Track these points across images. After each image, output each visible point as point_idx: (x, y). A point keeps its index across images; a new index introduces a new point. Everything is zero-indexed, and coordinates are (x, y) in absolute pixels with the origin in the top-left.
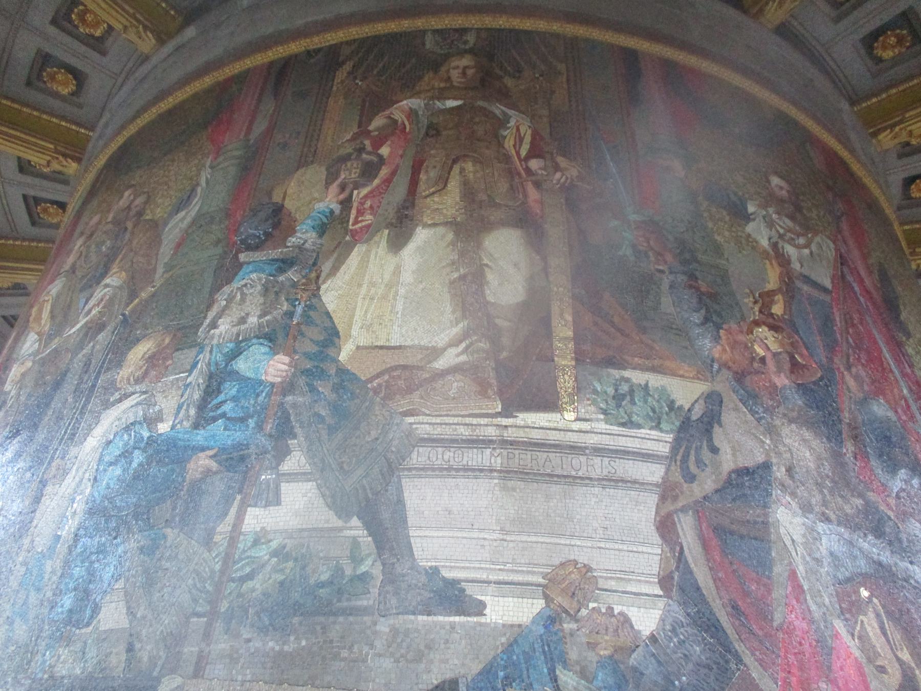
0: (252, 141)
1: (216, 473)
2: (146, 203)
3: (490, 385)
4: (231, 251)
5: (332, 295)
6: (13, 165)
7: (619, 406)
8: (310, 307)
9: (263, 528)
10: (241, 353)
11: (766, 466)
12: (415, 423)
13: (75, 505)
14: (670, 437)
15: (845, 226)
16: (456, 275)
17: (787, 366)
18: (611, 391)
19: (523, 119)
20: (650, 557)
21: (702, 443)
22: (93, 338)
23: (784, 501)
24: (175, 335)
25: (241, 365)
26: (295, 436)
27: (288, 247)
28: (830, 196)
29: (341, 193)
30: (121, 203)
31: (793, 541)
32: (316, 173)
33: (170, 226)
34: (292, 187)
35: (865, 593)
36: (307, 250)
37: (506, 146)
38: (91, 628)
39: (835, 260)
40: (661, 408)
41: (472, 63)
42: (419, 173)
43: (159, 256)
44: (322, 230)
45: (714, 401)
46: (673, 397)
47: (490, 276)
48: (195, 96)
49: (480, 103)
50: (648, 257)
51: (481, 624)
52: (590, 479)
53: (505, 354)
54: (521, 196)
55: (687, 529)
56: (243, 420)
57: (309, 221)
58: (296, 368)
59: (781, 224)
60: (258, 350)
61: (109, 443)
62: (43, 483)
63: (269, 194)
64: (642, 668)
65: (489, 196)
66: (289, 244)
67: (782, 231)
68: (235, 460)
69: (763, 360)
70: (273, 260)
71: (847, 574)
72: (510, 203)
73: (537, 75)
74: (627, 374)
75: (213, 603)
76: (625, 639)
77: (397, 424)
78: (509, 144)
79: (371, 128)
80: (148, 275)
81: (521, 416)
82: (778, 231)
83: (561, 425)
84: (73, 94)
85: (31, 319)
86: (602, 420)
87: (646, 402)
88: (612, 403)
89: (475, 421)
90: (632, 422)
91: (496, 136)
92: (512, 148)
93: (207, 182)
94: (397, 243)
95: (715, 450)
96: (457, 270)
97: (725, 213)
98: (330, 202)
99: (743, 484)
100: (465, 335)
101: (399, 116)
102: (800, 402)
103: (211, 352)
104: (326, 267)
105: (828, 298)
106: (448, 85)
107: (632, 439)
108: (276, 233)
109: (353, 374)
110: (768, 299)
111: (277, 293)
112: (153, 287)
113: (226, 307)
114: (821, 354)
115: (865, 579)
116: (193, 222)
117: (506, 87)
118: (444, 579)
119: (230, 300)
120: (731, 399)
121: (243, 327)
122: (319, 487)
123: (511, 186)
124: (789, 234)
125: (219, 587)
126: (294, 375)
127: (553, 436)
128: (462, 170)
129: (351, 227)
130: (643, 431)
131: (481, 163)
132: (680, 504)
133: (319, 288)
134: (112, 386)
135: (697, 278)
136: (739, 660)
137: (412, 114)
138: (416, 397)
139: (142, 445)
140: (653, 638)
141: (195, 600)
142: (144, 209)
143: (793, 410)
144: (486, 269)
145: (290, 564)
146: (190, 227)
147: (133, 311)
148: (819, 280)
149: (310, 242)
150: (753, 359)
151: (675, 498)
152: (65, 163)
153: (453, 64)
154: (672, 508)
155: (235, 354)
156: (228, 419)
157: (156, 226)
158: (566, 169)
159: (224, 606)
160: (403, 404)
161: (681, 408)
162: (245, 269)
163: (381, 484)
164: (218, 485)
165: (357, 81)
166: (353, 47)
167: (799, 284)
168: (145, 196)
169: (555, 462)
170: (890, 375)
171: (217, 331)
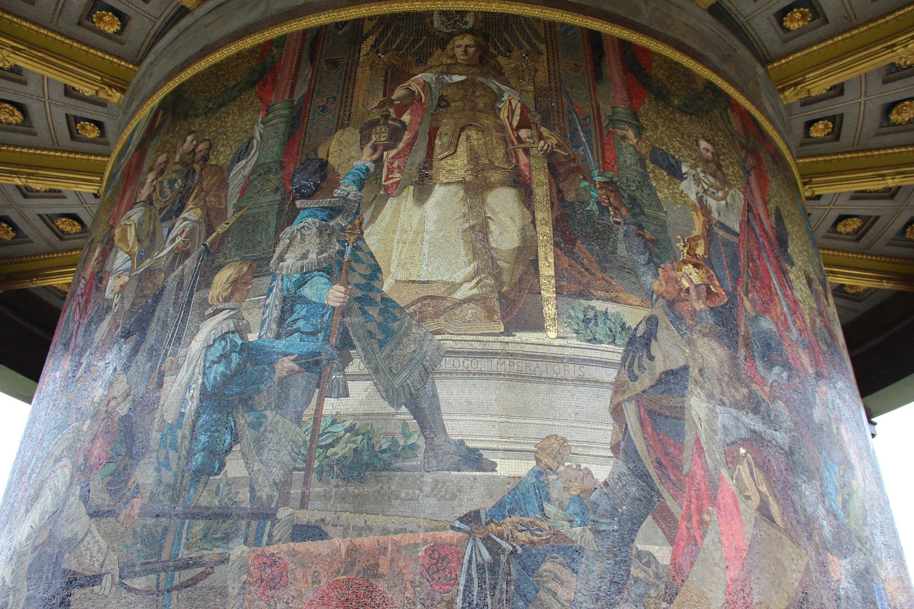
0: (295, 103)
1: (298, 372)
2: (209, 149)
3: (496, 312)
4: (289, 198)
5: (373, 238)
6: (61, 91)
8: (356, 248)
9: (337, 413)
11: (685, 368)
13: (192, 391)
14: (621, 350)
15: (753, 179)
16: (467, 225)
17: (704, 294)
18: (581, 316)
19: (513, 93)
20: (606, 432)
22: (182, 261)
23: (695, 393)
24: (251, 266)
26: (354, 348)
28: (743, 154)
29: (373, 154)
30: (185, 146)
32: (351, 135)
33: (234, 172)
34: (334, 146)
35: (742, 451)
37: (501, 117)
38: (221, 476)
39: (744, 210)
41: (472, 43)
42: (435, 139)
43: (228, 197)
45: (652, 321)
46: (624, 320)
47: (493, 227)
48: (239, 55)
49: (480, 79)
50: (609, 211)
51: (494, 477)
52: (566, 380)
53: (505, 288)
55: (631, 412)
57: (350, 177)
58: (350, 295)
60: (320, 281)
61: (210, 347)
62: (162, 375)
63: (315, 151)
64: (598, 502)
67: (706, 187)
68: (311, 363)
69: (688, 290)
70: (323, 207)
71: (733, 439)
72: (506, 166)
74: (593, 303)
75: (308, 461)
76: (588, 484)
78: (504, 115)
79: (393, 97)
80: (221, 214)
81: (518, 334)
83: (546, 342)
84: (117, 33)
85: (116, 238)
87: (605, 323)
88: (582, 325)
89: (485, 338)
90: (595, 339)
91: (493, 108)
93: (261, 136)
94: (422, 196)
95: (651, 358)
96: (468, 221)
97: (665, 174)
98: (365, 160)
99: (669, 381)
100: (477, 273)
101: (415, 87)
102: (711, 322)
103: (282, 280)
104: (367, 216)
105: (735, 240)
108: (325, 185)
111: (329, 235)
112: (227, 224)
113: (290, 245)
114: (729, 284)
115: (744, 442)
116: (253, 171)
117: (499, 63)
118: (468, 448)
119: (292, 239)
120: (664, 321)
121: (305, 262)
122: (375, 385)
123: (507, 152)
125: (310, 450)
127: (541, 350)
128: (468, 138)
131: (483, 131)
133: (362, 233)
134: (204, 303)
136: (660, 496)
137: (426, 86)
138: (441, 320)
139: (238, 350)
140: (606, 484)
141: (295, 461)
142: (208, 154)
143: (706, 328)
144: (490, 221)
145: (360, 437)
146: (251, 174)
147: (212, 243)
148: (731, 226)
149: (352, 194)
150: (681, 289)
151: (624, 392)
152: (110, 92)
153: (457, 43)
155: (301, 283)
156: (303, 333)
157: (222, 174)
159: (316, 464)
160: (432, 325)
161: (630, 328)
162: (302, 214)
164: (301, 380)
166: (374, 22)
167: (716, 229)
168: (207, 143)
169: (543, 368)
170: (776, 297)
171: (284, 264)
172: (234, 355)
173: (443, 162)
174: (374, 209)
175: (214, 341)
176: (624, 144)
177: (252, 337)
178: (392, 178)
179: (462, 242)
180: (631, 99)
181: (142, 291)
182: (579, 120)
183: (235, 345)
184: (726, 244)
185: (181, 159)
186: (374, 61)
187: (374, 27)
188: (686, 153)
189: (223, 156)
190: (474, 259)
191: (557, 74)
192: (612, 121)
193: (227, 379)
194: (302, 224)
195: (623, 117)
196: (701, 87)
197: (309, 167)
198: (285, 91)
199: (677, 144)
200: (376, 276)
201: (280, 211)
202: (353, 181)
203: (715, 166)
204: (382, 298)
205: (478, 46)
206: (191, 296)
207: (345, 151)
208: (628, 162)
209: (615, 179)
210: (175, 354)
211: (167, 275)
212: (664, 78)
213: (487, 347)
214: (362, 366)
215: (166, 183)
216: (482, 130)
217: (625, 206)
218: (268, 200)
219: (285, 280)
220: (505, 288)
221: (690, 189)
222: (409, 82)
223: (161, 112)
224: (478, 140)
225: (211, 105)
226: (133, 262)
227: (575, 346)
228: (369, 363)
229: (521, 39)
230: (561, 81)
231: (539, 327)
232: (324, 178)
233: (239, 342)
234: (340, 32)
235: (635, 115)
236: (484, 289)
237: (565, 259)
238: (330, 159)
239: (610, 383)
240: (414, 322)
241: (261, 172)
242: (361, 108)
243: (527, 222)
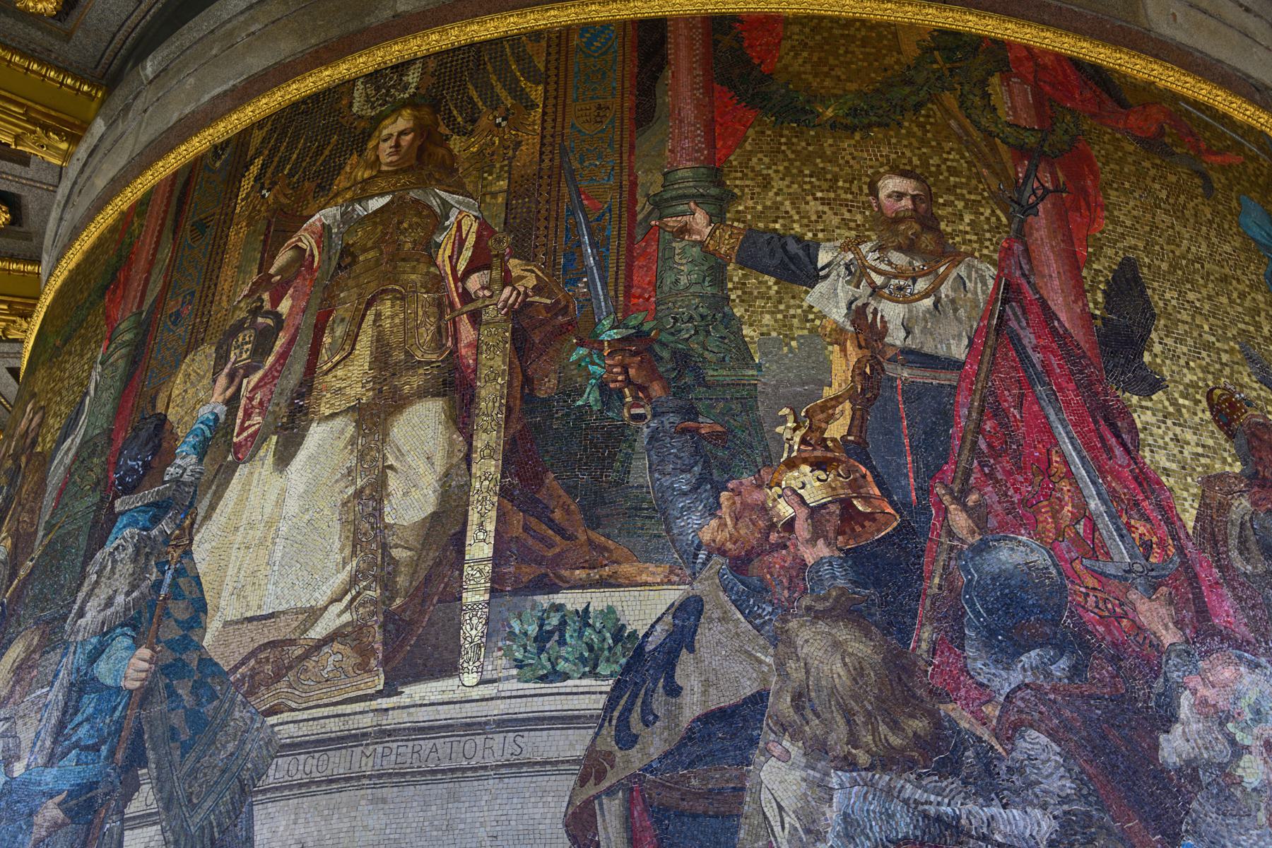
7: (541, 650)
8: (178, 573)
11: (759, 699)
12: (277, 725)
14: (607, 686)
16: (351, 491)
18: (533, 630)
23: (777, 750)
25: (103, 669)
31: (780, 808)
36: (184, 484)
44: (202, 450)
47: (394, 483)
49: (413, 194)
54: (449, 344)
56: (95, 748)
58: (156, 664)
65: (407, 352)
67: (879, 280)
69: (790, 525)
72: (434, 357)
73: (498, 120)
74: (559, 598)
78: (443, 256)
79: (272, 271)
81: (407, 690)
86: (513, 677)
87: (580, 636)
88: (532, 647)
89: (348, 709)
90: (555, 671)
95: (674, 691)
97: (771, 281)
100: (353, 581)
107: (552, 698)
109: (216, 664)
110: (822, 416)
119: (99, 573)
120: (718, 601)
121: (109, 612)
122: (163, 831)
123: (439, 328)
124: (893, 282)
127: (445, 713)
128: (378, 315)
129: (235, 440)
130: (569, 682)
132: (605, 784)
133: (191, 540)
138: (282, 686)
144: (389, 472)
150: (772, 526)
151: (599, 779)
153: (385, 132)
154: (593, 792)
158: (521, 278)
160: (266, 699)
161: (634, 634)
162: (123, 521)
163: (230, 818)
165: (264, 192)
173: (329, 378)
178: (250, 426)
180: (711, 144)
184: (914, 394)
188: (836, 220)
190: (354, 553)
194: (115, 545)
199: (813, 207)
204: (201, 660)
208: (684, 281)
221: (831, 300)
227: (516, 694)
229: (499, 88)
231: (448, 668)
235: (715, 174)
236: (361, 610)
237: (518, 519)
239: (574, 762)
242: (224, 304)
243: (455, 460)
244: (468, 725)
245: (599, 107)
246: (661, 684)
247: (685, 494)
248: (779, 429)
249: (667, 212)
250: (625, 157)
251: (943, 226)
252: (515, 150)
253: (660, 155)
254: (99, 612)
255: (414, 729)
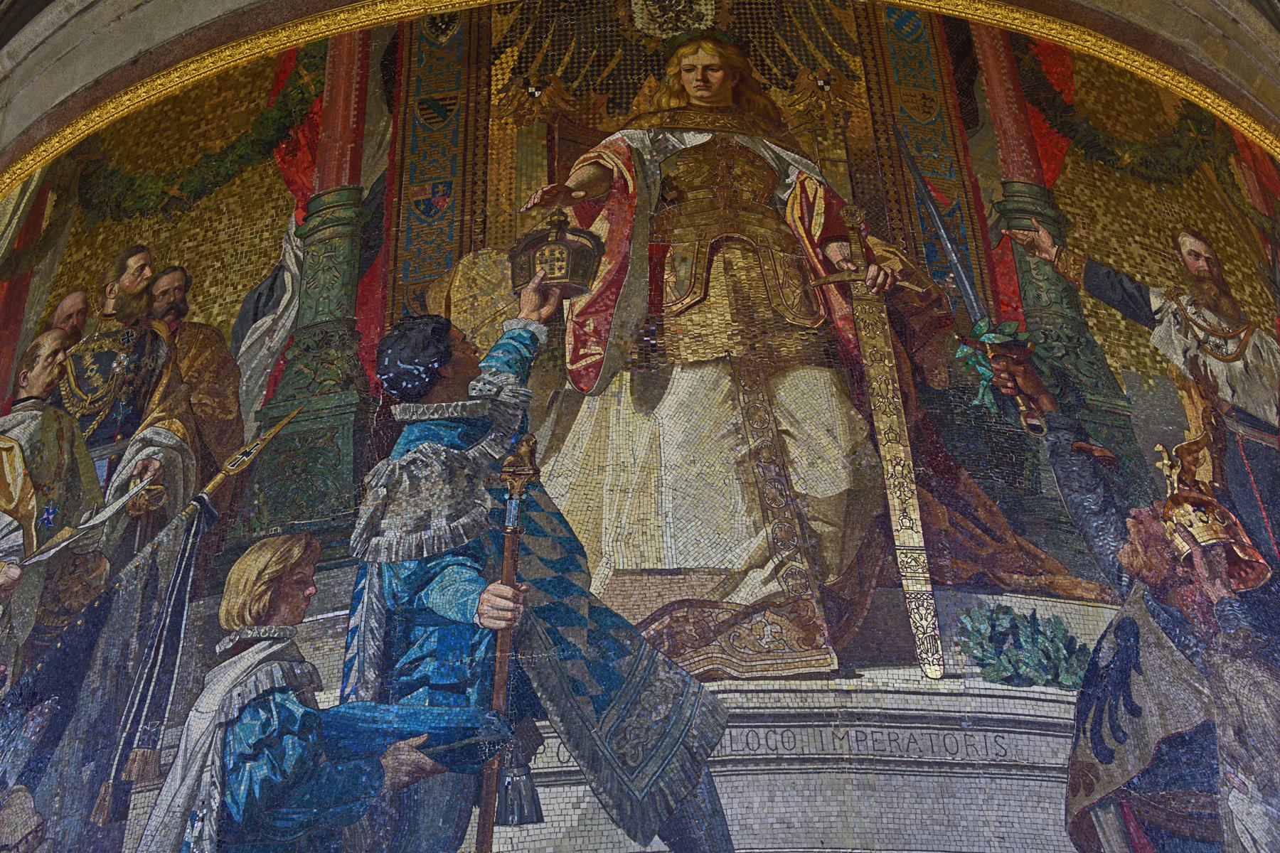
0: (366, 193)
1: (434, 772)
3: (818, 628)
4: (376, 400)
7: (999, 652)
8: (525, 505)
10: (432, 579)
11: (1207, 728)
12: (719, 692)
13: (198, 825)
14: (1072, 696)
16: (744, 450)
17: (1223, 566)
18: (985, 628)
19: (805, 166)
21: (1117, 700)
24: (308, 545)
25: (435, 598)
26: (545, 716)
27: (472, 398)
29: (542, 306)
30: (126, 279)
31: (1253, 839)
32: (489, 266)
37: (789, 219)
40: (1058, 650)
41: (716, 61)
43: (242, 397)
44: (524, 370)
45: (1124, 629)
47: (794, 451)
48: (224, 78)
49: (738, 139)
50: (1017, 406)
52: (972, 766)
53: (832, 578)
54: (822, 312)
56: (458, 690)
57: (499, 353)
58: (525, 604)
59: (1200, 321)
60: (458, 576)
63: (421, 299)
65: (774, 311)
66: (473, 393)
67: (1201, 335)
69: (1189, 558)
70: (450, 419)
72: (808, 323)
73: (821, 83)
74: (1005, 600)
77: (694, 694)
78: (793, 213)
80: (231, 433)
81: (867, 674)
82: (1196, 336)
83: (924, 686)
87: (1034, 642)
89: (804, 685)
91: (772, 200)
92: (799, 223)
93: (300, 264)
94: (649, 393)
95: (1135, 711)
96: (744, 441)
98: (527, 318)
99: (1177, 759)
100: (773, 548)
101: (612, 162)
103: (380, 575)
104: (543, 435)
106: (683, 104)
107: (1022, 702)
108: (448, 371)
109: (617, 615)
110: (1190, 458)
112: (246, 454)
113: (388, 500)
116: (291, 340)
117: (773, 103)
119: (392, 485)
120: (1150, 628)
121: (425, 535)
123: (806, 292)
124: (1212, 339)
126: (526, 616)
127: (914, 703)
128: (728, 265)
130: (1035, 688)
131: (755, 251)
132: (1097, 797)
133: (537, 472)
134: (211, 629)
135: (1087, 435)
137: (632, 156)
142: (184, 300)
143: (1235, 639)
144: (787, 439)
146: (287, 348)
147: (215, 495)
148: (1260, 415)
150: (1175, 559)
151: (1090, 789)
153: (685, 62)
154: (1086, 803)
155: (421, 580)
160: (696, 662)
163: (685, 787)
165: (531, 90)
166: (512, 17)
167: (1231, 425)
168: (178, 274)
171: (383, 541)
172: (288, 740)
173: (682, 320)
174: (557, 422)
175: (242, 710)
176: (1032, 260)
177: (327, 700)
178: (586, 356)
179: (737, 486)
180: (1037, 162)
181: (57, 600)
182: (940, 216)
183: (287, 718)
184: (1254, 452)
185: (119, 307)
186: (521, 105)
187: (512, 29)
188: (1156, 268)
189: (217, 306)
190: (765, 519)
191: (890, 120)
192: (1004, 213)
193: (275, 795)
194: (408, 457)
195: (1026, 202)
196: (1173, 117)
197: (414, 333)
198: (340, 168)
200: (573, 561)
201: (360, 428)
202: (507, 363)
203: (1212, 287)
204: (592, 609)
205: (726, 66)
206: (177, 613)
207: (482, 300)
208: (1045, 298)
209: (1023, 336)
210: (151, 740)
211: (116, 567)
212: (1100, 107)
213: (809, 703)
214: (565, 754)
215: (88, 359)
216: (750, 249)
217: (1046, 392)
218: (332, 404)
219: (386, 575)
220: (832, 578)
221: (1170, 344)
222: (598, 148)
223: (52, 197)
224: (748, 270)
225: (174, 191)
226: (27, 535)
227: (980, 693)
228: (577, 747)
229: (811, 47)
230: (898, 134)
231: (907, 657)
232: (445, 357)
233: (299, 711)
234: (443, 39)
235: (1048, 196)
238: (453, 316)
239: (1061, 770)
240: (661, 657)
241: (310, 342)
242: (506, 207)
243: (859, 439)
244: (942, 718)
245: (924, 97)
246: (1121, 702)
247: (1095, 514)
248: (1159, 464)
249: (1015, 222)
250: (961, 155)
251: (1233, 292)
252: (846, 120)
253: (995, 163)
254: (408, 533)
255: (885, 716)
